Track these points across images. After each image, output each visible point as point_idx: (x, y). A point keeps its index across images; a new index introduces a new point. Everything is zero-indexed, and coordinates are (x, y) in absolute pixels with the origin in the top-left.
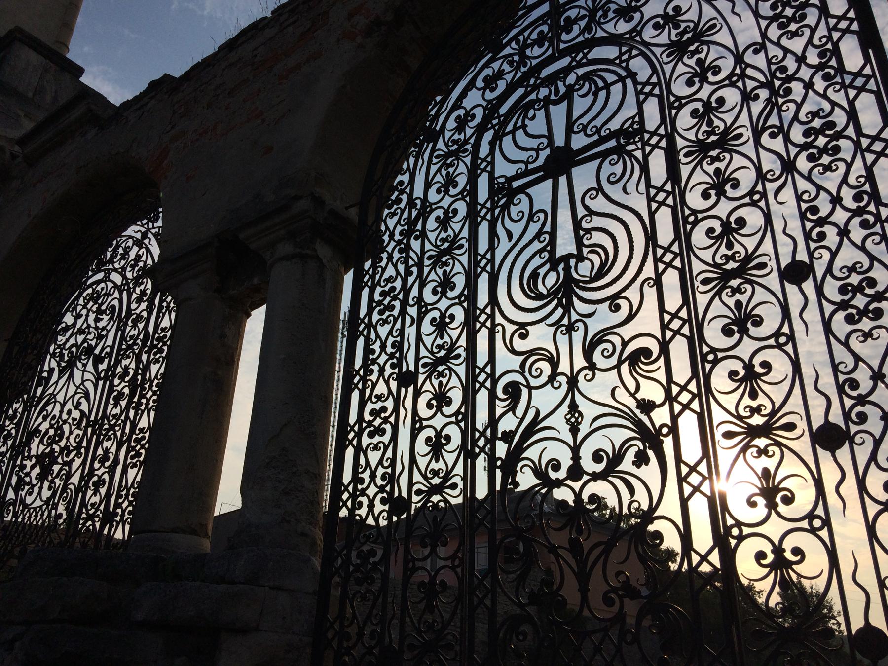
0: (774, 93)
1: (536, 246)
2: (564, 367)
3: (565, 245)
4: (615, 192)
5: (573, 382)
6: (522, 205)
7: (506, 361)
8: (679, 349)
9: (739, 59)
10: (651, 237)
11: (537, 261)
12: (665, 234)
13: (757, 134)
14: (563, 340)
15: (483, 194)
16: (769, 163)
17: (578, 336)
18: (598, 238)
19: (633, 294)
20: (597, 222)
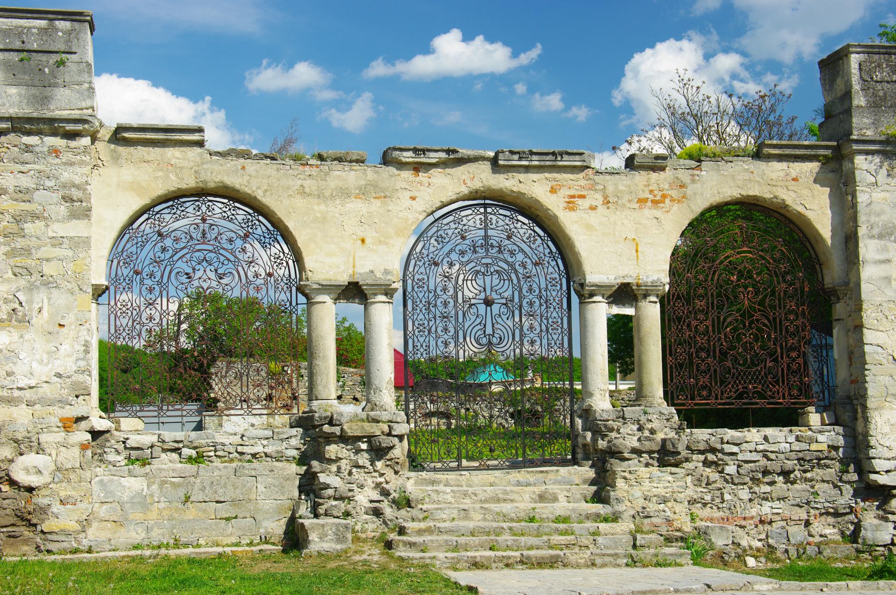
0: (547, 307)
1: (479, 327)
3: (489, 330)
4: (505, 318)
6: (473, 310)
9: (540, 292)
11: (479, 333)
12: (517, 338)
13: (542, 316)
15: (460, 300)
16: (544, 327)
18: (499, 331)
19: (508, 352)
20: (499, 326)
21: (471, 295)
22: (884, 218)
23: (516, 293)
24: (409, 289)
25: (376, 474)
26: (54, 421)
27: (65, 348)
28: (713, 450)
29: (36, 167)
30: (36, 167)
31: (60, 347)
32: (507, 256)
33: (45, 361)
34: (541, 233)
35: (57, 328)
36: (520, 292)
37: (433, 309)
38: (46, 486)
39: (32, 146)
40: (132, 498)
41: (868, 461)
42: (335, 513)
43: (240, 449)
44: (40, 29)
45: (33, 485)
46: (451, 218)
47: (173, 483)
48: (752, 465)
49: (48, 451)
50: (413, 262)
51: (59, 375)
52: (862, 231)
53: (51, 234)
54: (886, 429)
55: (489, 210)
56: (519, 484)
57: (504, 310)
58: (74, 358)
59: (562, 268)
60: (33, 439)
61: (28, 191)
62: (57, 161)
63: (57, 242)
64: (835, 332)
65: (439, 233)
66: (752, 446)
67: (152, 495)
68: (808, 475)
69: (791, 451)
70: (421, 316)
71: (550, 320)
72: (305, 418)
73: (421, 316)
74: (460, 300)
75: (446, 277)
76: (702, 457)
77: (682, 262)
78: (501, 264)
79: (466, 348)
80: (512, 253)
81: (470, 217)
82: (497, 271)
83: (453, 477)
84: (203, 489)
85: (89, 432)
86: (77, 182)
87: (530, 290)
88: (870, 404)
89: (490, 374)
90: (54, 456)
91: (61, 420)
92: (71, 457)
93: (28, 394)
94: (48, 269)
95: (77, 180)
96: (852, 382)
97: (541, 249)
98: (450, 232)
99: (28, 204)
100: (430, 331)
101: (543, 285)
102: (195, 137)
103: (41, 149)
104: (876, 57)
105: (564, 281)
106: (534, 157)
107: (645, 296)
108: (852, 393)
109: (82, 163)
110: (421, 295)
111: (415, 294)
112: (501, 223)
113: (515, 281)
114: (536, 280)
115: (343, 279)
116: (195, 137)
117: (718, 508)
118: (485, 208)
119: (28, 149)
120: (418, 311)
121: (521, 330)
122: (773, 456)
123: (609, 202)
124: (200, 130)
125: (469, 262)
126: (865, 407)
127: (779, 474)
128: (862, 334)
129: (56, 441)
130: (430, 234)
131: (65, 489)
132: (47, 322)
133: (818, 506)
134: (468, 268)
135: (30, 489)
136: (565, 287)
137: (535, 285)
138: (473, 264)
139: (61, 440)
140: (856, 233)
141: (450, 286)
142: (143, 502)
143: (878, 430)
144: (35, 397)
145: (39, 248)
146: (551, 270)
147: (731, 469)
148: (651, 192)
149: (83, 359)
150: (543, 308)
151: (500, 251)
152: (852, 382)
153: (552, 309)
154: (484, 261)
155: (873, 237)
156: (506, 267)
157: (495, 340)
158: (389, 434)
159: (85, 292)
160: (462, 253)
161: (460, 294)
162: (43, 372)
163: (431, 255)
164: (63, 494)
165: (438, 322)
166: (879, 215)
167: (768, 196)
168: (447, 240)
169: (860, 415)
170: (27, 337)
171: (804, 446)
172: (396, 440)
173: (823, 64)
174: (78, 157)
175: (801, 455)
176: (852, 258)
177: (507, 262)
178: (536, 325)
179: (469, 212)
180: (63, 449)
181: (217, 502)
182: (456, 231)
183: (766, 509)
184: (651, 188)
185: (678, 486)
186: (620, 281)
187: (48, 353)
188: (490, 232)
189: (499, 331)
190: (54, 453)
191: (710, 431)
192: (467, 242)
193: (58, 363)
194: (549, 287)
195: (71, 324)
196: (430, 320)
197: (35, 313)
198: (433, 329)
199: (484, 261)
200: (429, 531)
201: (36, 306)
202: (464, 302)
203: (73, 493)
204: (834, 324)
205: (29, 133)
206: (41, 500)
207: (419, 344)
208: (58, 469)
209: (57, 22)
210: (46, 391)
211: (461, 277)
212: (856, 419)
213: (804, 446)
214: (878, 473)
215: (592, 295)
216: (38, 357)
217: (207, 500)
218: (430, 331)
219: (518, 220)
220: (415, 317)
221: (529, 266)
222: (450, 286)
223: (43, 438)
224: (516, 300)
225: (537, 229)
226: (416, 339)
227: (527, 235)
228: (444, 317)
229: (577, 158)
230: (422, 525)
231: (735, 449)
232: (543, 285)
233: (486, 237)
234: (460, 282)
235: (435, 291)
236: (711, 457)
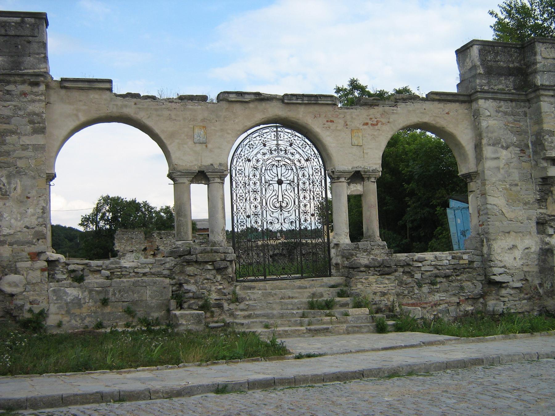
1: (274, 197)
2: (280, 221)
3: (280, 199)
4: (289, 192)
5: (282, 224)
6: (271, 187)
7: (269, 218)
8: (298, 222)
9: (309, 176)
10: (295, 204)
13: (310, 191)
14: (280, 216)
15: (263, 182)
16: (312, 197)
17: (282, 216)
18: (286, 200)
19: (291, 211)
20: (286, 196)
21: (270, 179)
22: (495, 134)
23: (296, 178)
24: (234, 175)
25: (217, 284)
26: (25, 254)
27: (31, 211)
28: (408, 265)
29: (14, 103)
30: (14, 103)
31: (27, 210)
32: (290, 156)
33: (19, 218)
34: (309, 143)
35: (26, 199)
36: (298, 176)
37: (248, 187)
38: (21, 293)
39: (10, 91)
40: (73, 300)
41: (490, 269)
42: (194, 307)
43: (136, 270)
44: (16, 23)
45: (13, 293)
46: (257, 134)
47: (97, 291)
48: (429, 273)
49: (22, 272)
50: (235, 160)
51: (27, 227)
52: (484, 141)
53: (22, 143)
54: (499, 251)
55: (279, 129)
56: (300, 288)
57: (289, 187)
58: (36, 217)
59: (321, 163)
60: (13, 265)
61: (9, 117)
62: (25, 100)
63: (25, 148)
64: (470, 198)
65: (251, 143)
66: (428, 263)
67: (84, 298)
68: (459, 278)
69: (450, 264)
70: (241, 191)
71: (315, 193)
72: (174, 251)
73: (241, 191)
74: (263, 182)
75: (254, 168)
76: (401, 270)
77: (387, 160)
78: (286, 160)
79: (267, 209)
80: (292, 154)
81: (268, 133)
82: (284, 165)
83: (262, 284)
84: (114, 294)
85: (46, 261)
86: (37, 112)
87: (304, 175)
88: (492, 237)
89: (282, 224)
90: (25, 276)
91: (29, 254)
92: (35, 276)
93: (9, 239)
94: (20, 163)
95: (37, 110)
96: (480, 225)
97: (309, 152)
98: (257, 142)
99: (8, 125)
100: (246, 200)
101: (311, 173)
102: (107, 86)
103: (16, 93)
104: (487, 48)
105: (323, 170)
106: (305, 99)
107: (369, 178)
108: (480, 232)
109: (40, 101)
110: (240, 179)
111: (237, 179)
112: (286, 137)
113: (295, 170)
114: (307, 170)
115: (196, 169)
116: (107, 86)
117: (412, 298)
118: (277, 128)
119: (8, 92)
120: (239, 188)
121: (299, 198)
122: (440, 268)
123: (347, 125)
124: (110, 81)
125: (268, 159)
126: (488, 240)
127: (443, 278)
128: (486, 199)
129: (27, 266)
130: (245, 143)
131: (33, 295)
132: (20, 195)
133: (464, 295)
134: (268, 163)
135: (12, 295)
136: (323, 174)
137: (306, 173)
138: (270, 161)
139: (29, 266)
140: (481, 143)
141: (257, 173)
142: (78, 303)
143: (495, 252)
144: (13, 240)
145: (15, 151)
146: (315, 164)
147: (418, 276)
148: (371, 119)
149: (42, 217)
150: (311, 185)
151: (286, 153)
152: (480, 225)
153: (316, 186)
154: (277, 159)
155: (490, 145)
156: (289, 162)
157: (284, 205)
158: (224, 260)
159: (42, 177)
160: (264, 154)
161: (263, 178)
162: (18, 225)
163: (246, 156)
164: (31, 298)
165: (251, 194)
166: (492, 133)
167: (433, 122)
168: (255, 146)
169: (485, 243)
170: (7, 204)
171: (456, 261)
172: (228, 263)
173: (458, 52)
174: (38, 98)
175: (455, 267)
176: (479, 157)
177: (290, 159)
178: (307, 195)
179: (268, 130)
180: (30, 271)
181: (123, 302)
182: (260, 142)
183: (437, 297)
184: (370, 117)
185: (391, 286)
186: (355, 169)
187: (21, 214)
188: (280, 142)
189: (286, 200)
190: (25, 273)
191: (406, 254)
192: (267, 148)
193: (26, 219)
194: (314, 174)
195: (34, 197)
196: (246, 193)
197: (12, 190)
198: (248, 199)
199: (277, 159)
200: (249, 316)
201: (13, 186)
202: (265, 182)
203: (37, 298)
204: (469, 193)
205: (9, 83)
206: (19, 302)
207: (240, 208)
208: (28, 283)
209: (26, 19)
210: (19, 236)
211: (264, 168)
212: (483, 246)
213: (456, 261)
214: (495, 275)
215: (338, 178)
216: (14, 216)
217: (117, 300)
218: (246, 200)
219: (296, 135)
220: (237, 191)
221: (303, 161)
222: (257, 173)
223: (19, 265)
224: (296, 181)
225: (307, 140)
226: (238, 205)
227: (301, 144)
228: (255, 191)
229: (329, 99)
230: (246, 313)
231: (420, 265)
232: (311, 173)
233: (278, 145)
234: (263, 171)
235: (249, 176)
236: (407, 269)
